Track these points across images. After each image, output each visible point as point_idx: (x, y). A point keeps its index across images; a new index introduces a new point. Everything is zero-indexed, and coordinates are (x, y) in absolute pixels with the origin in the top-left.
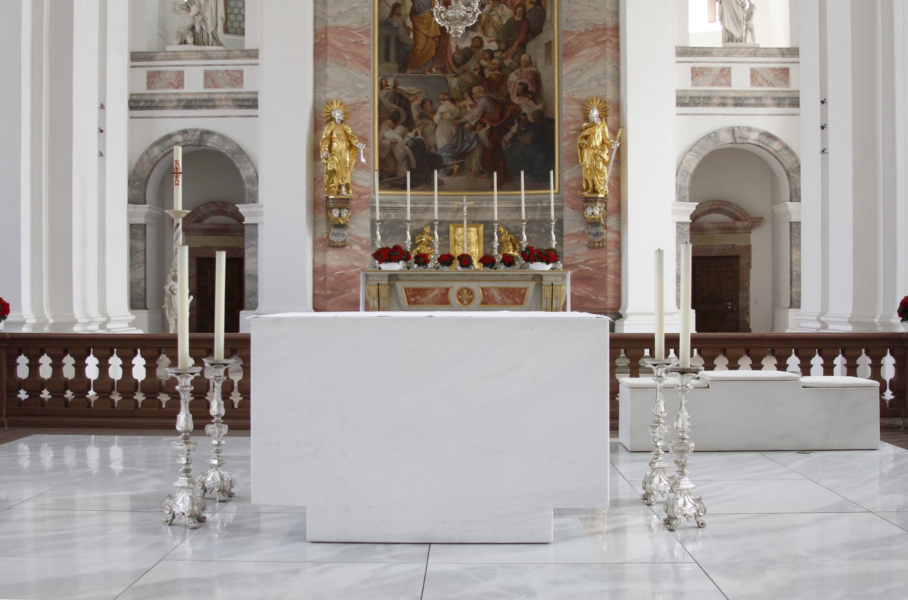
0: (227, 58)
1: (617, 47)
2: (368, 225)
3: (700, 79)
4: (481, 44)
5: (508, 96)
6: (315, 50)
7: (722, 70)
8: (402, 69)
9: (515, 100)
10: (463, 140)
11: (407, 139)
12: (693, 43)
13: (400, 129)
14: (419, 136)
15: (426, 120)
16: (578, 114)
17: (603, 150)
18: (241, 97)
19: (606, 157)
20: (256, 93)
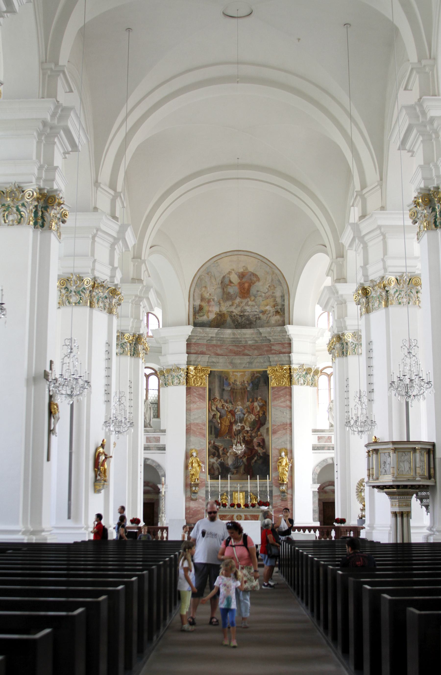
0: (154, 432)
1: (291, 430)
2: (205, 492)
3: (321, 440)
4: (244, 428)
5: (253, 447)
6: (186, 431)
7: (329, 437)
8: (216, 437)
9: (256, 448)
10: (238, 462)
11: (218, 462)
12: (318, 428)
13: (215, 458)
14: (222, 461)
15: (224, 455)
16: (278, 454)
17: (286, 467)
18: (159, 446)
19: (287, 469)
20: (165, 445)
